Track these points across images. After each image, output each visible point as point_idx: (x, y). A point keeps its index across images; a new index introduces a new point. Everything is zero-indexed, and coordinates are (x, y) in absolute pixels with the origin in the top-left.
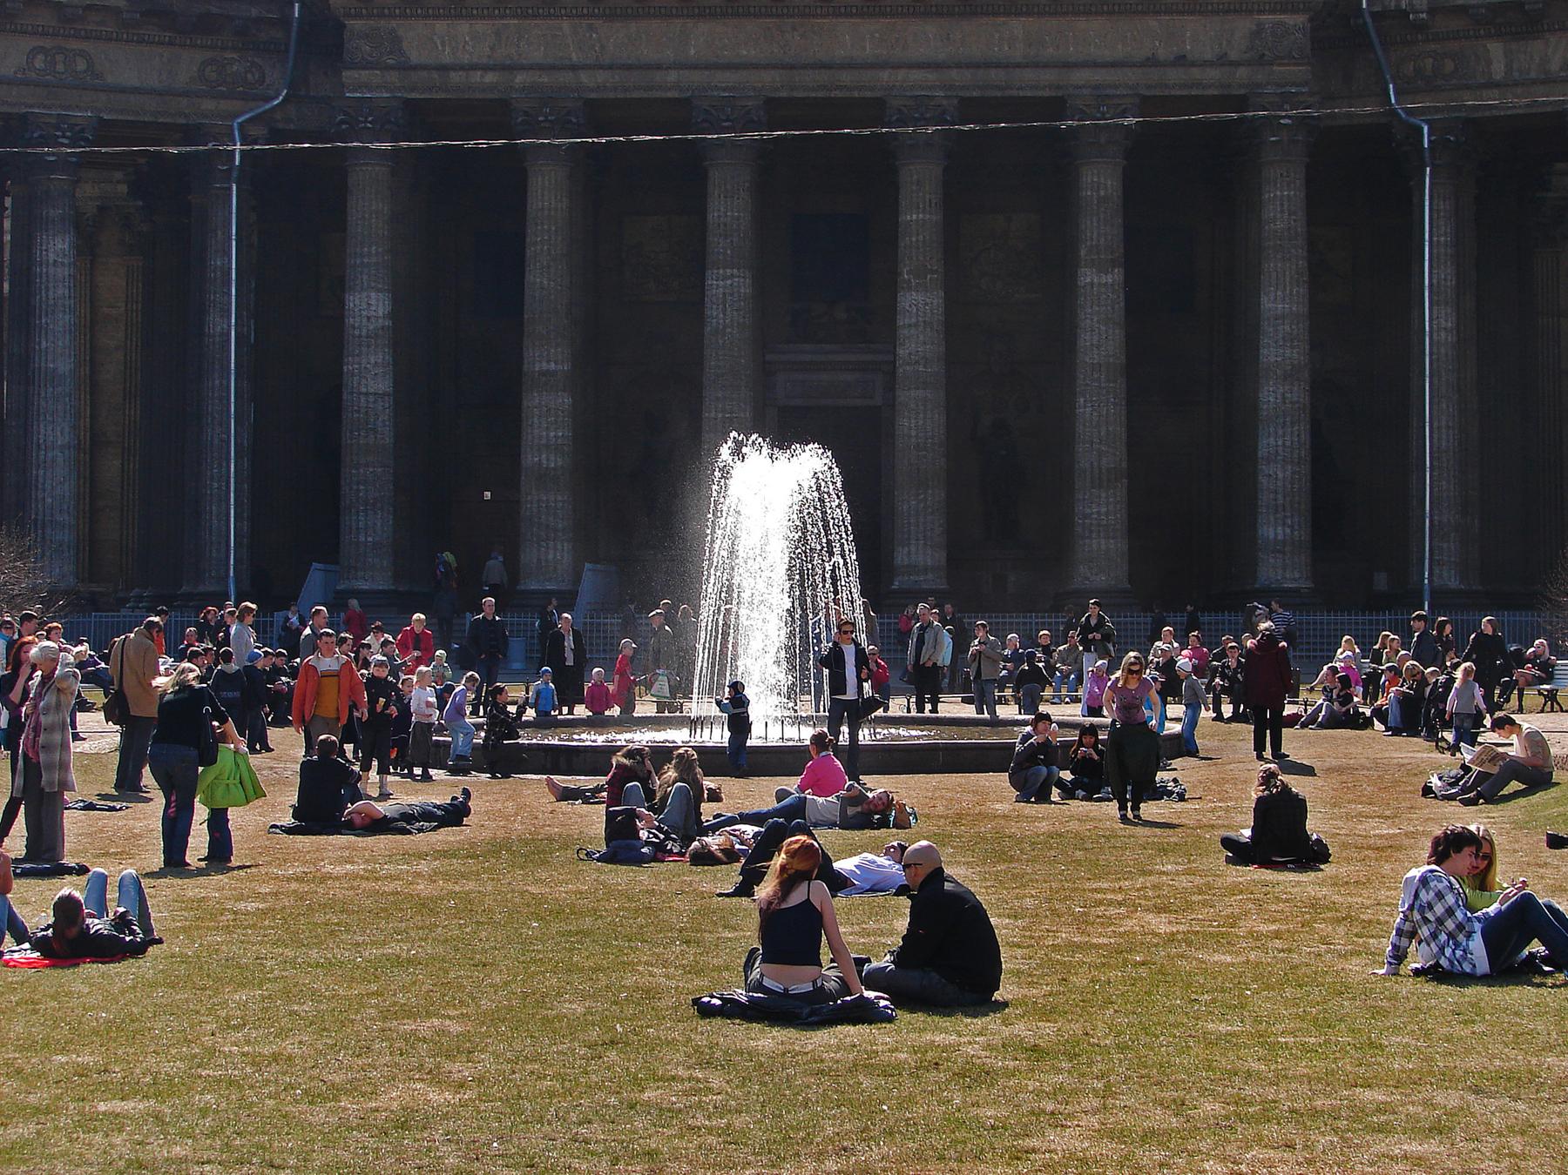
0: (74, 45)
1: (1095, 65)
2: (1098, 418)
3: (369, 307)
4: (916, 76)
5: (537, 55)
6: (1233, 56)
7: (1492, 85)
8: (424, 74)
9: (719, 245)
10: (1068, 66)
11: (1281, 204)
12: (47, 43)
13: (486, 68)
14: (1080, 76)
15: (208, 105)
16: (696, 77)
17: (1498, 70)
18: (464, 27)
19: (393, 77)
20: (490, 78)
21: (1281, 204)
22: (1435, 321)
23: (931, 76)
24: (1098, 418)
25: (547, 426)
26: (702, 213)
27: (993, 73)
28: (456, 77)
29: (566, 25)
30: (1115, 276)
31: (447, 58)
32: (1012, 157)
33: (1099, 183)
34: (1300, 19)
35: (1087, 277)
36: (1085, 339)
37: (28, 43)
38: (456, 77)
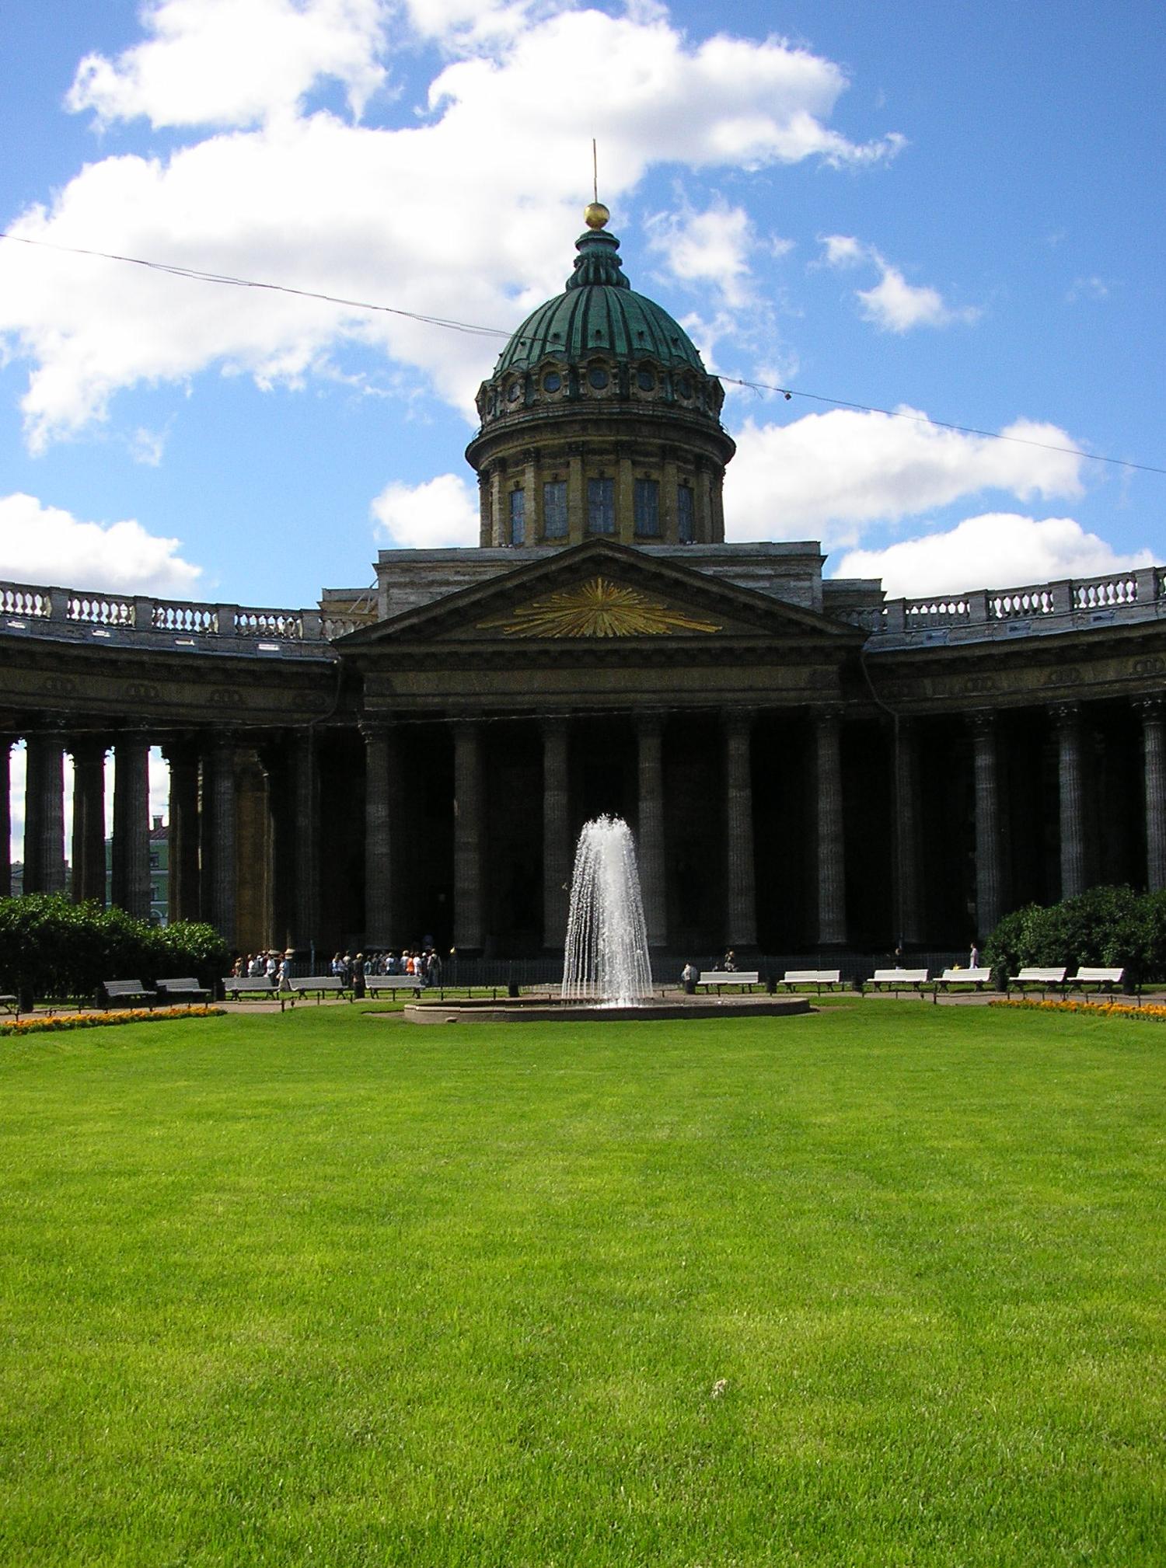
0: (232, 688)
1: (734, 690)
2: (739, 861)
3: (377, 812)
4: (646, 696)
5: (460, 689)
6: (802, 685)
7: (927, 699)
8: (404, 699)
9: (550, 780)
10: (720, 690)
11: (826, 755)
12: (221, 688)
13: (434, 695)
14: (729, 696)
15: (296, 716)
16: (540, 698)
17: (929, 692)
18: (423, 676)
19: (389, 700)
20: (437, 700)
21: (826, 755)
22: (904, 816)
23: (652, 696)
24: (739, 861)
25: (467, 871)
26: (541, 765)
27: (684, 695)
28: (419, 700)
29: (473, 674)
30: (747, 793)
31: (415, 689)
32: (693, 736)
33: (737, 747)
34: (834, 668)
35: (733, 793)
36: (733, 823)
37: (211, 688)
38: (419, 700)
